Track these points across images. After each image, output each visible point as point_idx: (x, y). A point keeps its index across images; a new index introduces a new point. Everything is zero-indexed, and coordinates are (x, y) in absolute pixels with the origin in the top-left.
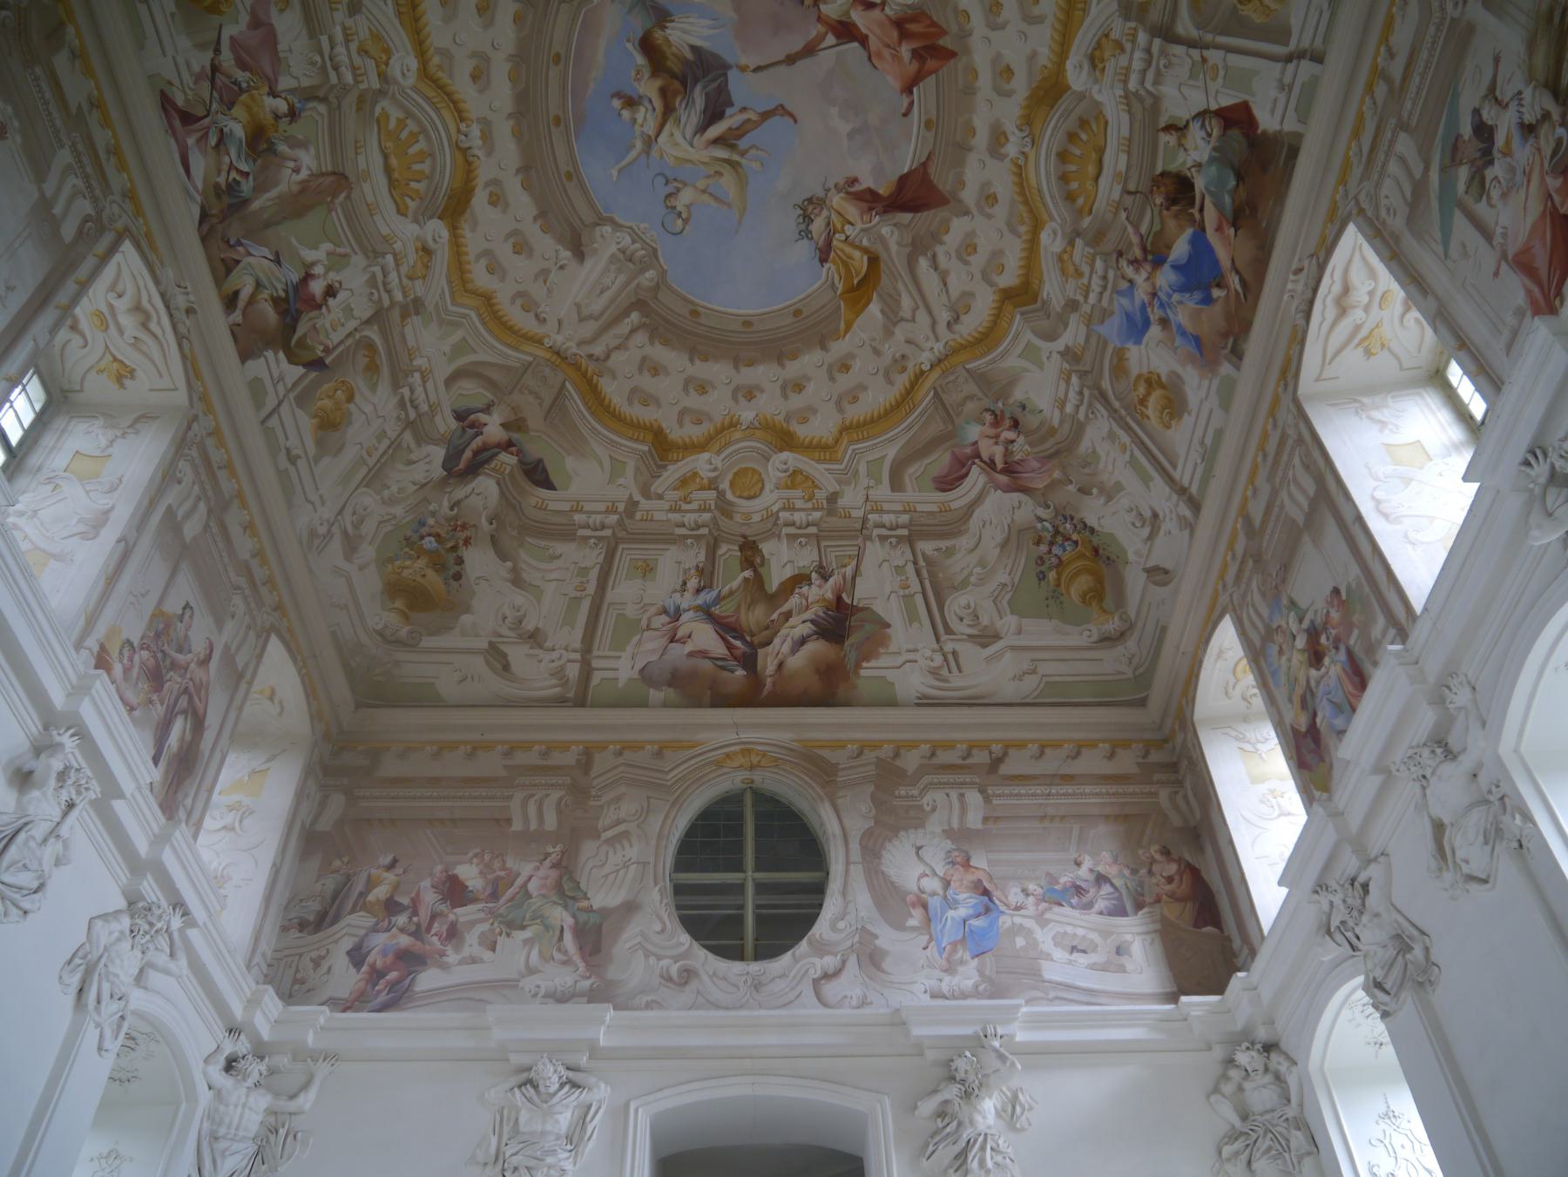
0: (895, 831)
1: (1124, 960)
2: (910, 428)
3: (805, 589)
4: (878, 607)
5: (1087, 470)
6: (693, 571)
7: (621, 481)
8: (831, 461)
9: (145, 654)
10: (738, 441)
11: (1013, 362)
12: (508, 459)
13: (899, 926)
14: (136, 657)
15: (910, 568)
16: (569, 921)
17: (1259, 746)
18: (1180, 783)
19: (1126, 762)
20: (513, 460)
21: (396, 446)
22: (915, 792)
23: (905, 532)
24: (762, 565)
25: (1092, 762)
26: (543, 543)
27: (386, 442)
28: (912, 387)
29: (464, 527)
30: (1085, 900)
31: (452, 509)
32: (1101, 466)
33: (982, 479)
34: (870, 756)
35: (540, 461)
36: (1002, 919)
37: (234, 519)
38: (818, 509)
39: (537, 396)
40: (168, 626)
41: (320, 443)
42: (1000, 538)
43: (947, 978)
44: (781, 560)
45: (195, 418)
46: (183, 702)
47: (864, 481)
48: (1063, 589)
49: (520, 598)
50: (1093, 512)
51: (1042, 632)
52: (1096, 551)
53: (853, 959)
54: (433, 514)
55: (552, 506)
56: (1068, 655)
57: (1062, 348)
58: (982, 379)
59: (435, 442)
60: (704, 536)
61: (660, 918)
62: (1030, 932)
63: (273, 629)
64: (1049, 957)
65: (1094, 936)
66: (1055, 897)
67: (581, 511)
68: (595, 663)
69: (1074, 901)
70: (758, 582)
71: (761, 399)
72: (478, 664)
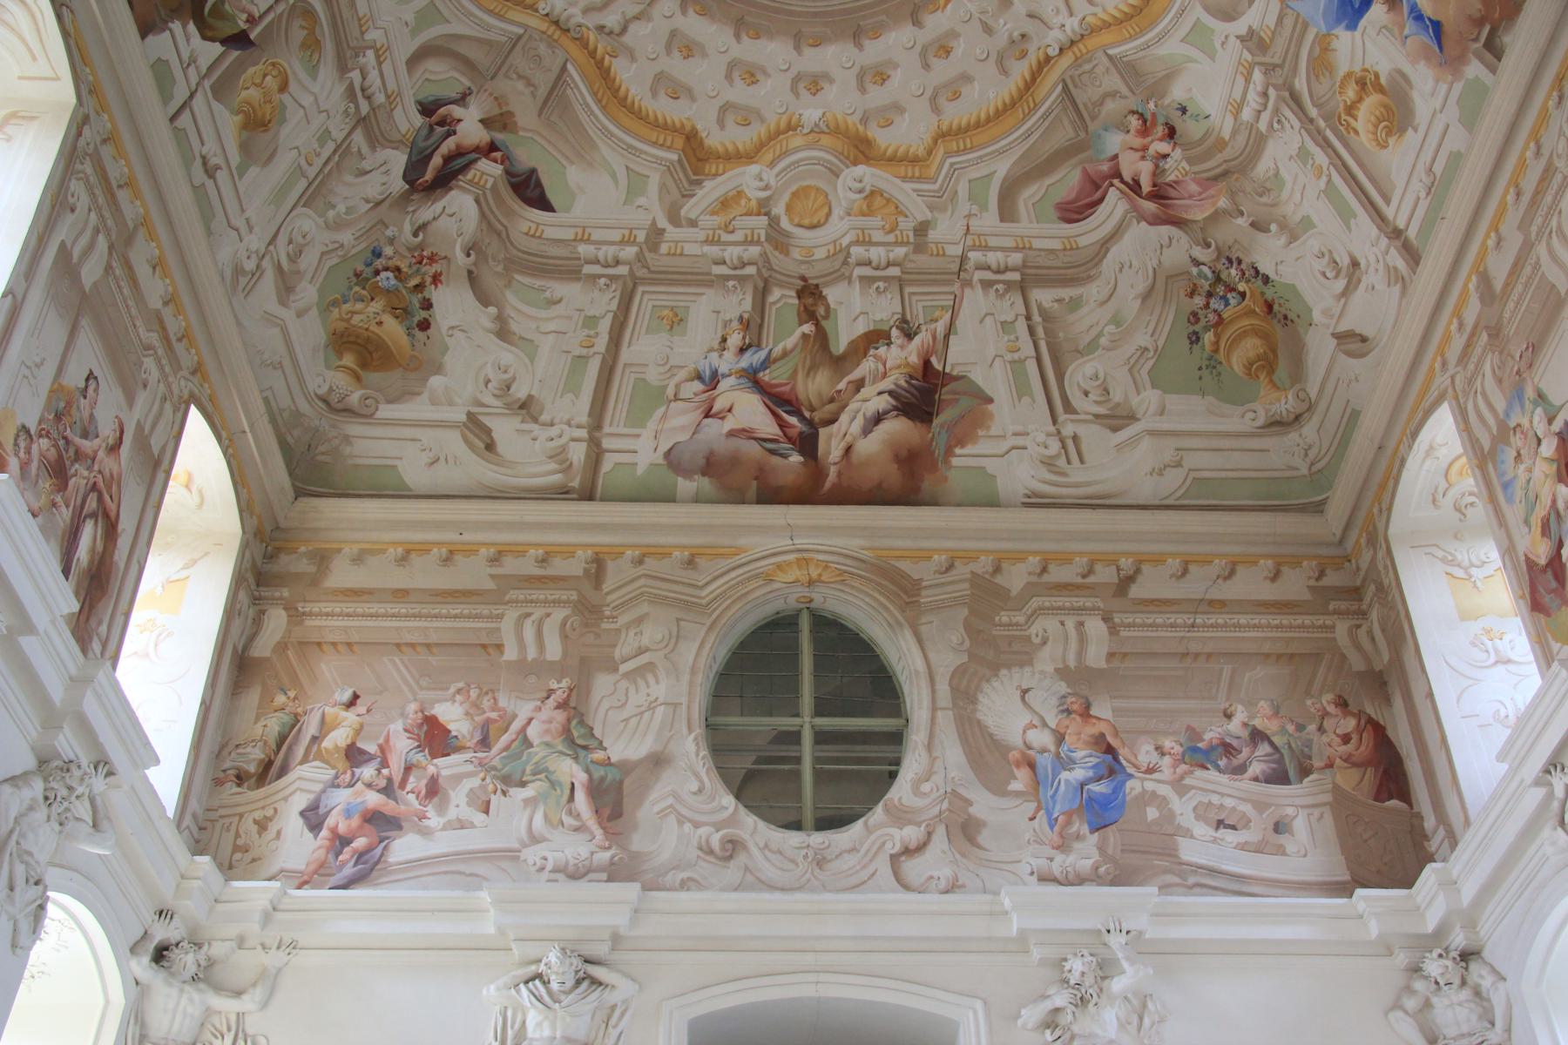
0: (995, 668)
1: (1283, 839)
2: (1028, 134)
3: (882, 350)
4: (978, 377)
5: (1264, 200)
6: (735, 324)
7: (642, 201)
8: (920, 179)
9: (44, 443)
10: (797, 150)
11: (1172, 48)
12: (489, 169)
13: (1000, 790)
14: (35, 447)
15: (1021, 325)
16: (581, 777)
17: (1474, 571)
18: (1364, 614)
19: (1295, 585)
20: (496, 170)
21: (343, 150)
22: (1021, 619)
23: (1016, 276)
24: (826, 317)
25: (1250, 585)
26: (538, 283)
27: (331, 146)
28: (1034, 79)
29: (432, 259)
30: (1236, 762)
31: (415, 235)
32: (1285, 195)
33: (1122, 206)
34: (962, 570)
35: (533, 171)
36: (1129, 784)
37: (141, 254)
38: (902, 244)
39: (529, 83)
40: (69, 404)
41: (245, 148)
42: (1141, 286)
43: (1059, 858)
44: (853, 308)
45: (86, 120)
46: (92, 503)
47: (964, 207)
48: (1221, 356)
49: (508, 355)
50: (1268, 254)
51: (1192, 412)
52: (1269, 306)
53: (941, 831)
54: (391, 241)
55: (550, 233)
56: (1216, 443)
57: (1243, 31)
58: (1129, 70)
59: (395, 145)
60: (750, 277)
61: (696, 775)
62: (1162, 802)
63: (193, 399)
64: (1188, 834)
65: (1247, 808)
66: (1199, 755)
67: (588, 241)
69: (1222, 763)
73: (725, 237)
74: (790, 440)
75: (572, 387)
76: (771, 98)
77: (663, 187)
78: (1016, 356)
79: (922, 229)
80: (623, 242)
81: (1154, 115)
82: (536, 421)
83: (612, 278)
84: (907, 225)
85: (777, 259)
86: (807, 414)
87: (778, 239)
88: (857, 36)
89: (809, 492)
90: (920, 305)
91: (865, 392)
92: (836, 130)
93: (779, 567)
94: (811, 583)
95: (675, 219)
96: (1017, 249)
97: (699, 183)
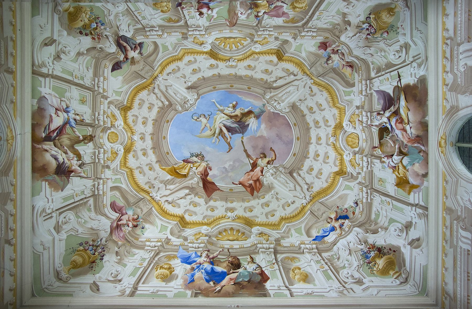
3: (76, 159)
4: (69, 186)
6: (82, 118)
10: (127, 134)
15: (83, 196)
24: (84, 143)
38: (104, 162)
42: (94, 227)
44: (86, 150)
49: (73, 54)
68: (47, 79)
70: (78, 142)
71: (141, 142)
72: (47, 34)
73: (105, 116)
74: (49, 133)
75: (64, 71)
76: (139, 128)
77: (118, 100)
78: (75, 196)
79: (108, 167)
80: (104, 89)
81: (139, 221)
82: (54, 59)
83: (94, 85)
84: (109, 163)
85: (100, 130)
86: (57, 138)
87: (105, 130)
88: (153, 148)
89: (35, 140)
90: (88, 168)
91: (64, 154)
92: (132, 144)
93: (11, 130)
94: (7, 140)
95: (110, 103)
96: (103, 192)
97: (119, 110)
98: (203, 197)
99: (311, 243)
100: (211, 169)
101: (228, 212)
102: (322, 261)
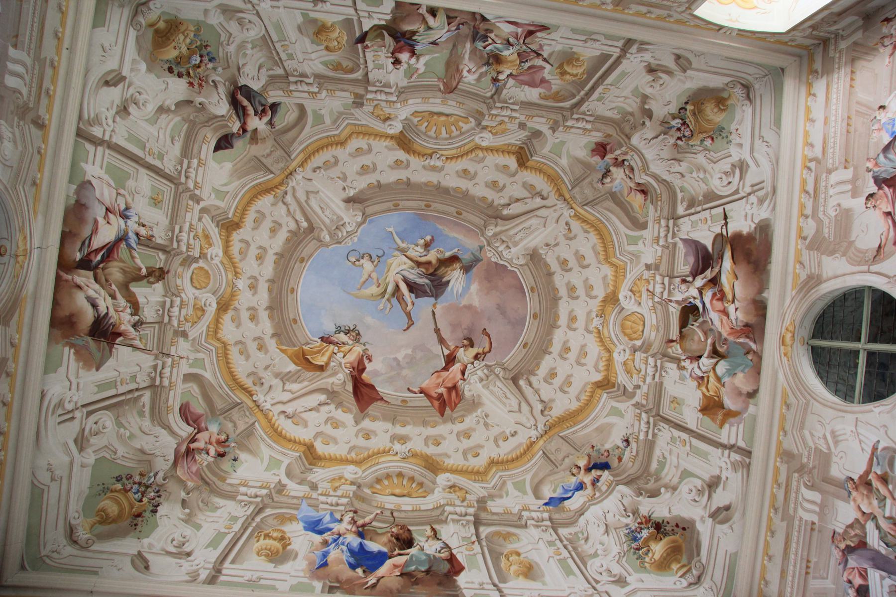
98: (349, 411)
99: (541, 509)
100: (370, 360)
101: (396, 442)
102: (558, 542)
